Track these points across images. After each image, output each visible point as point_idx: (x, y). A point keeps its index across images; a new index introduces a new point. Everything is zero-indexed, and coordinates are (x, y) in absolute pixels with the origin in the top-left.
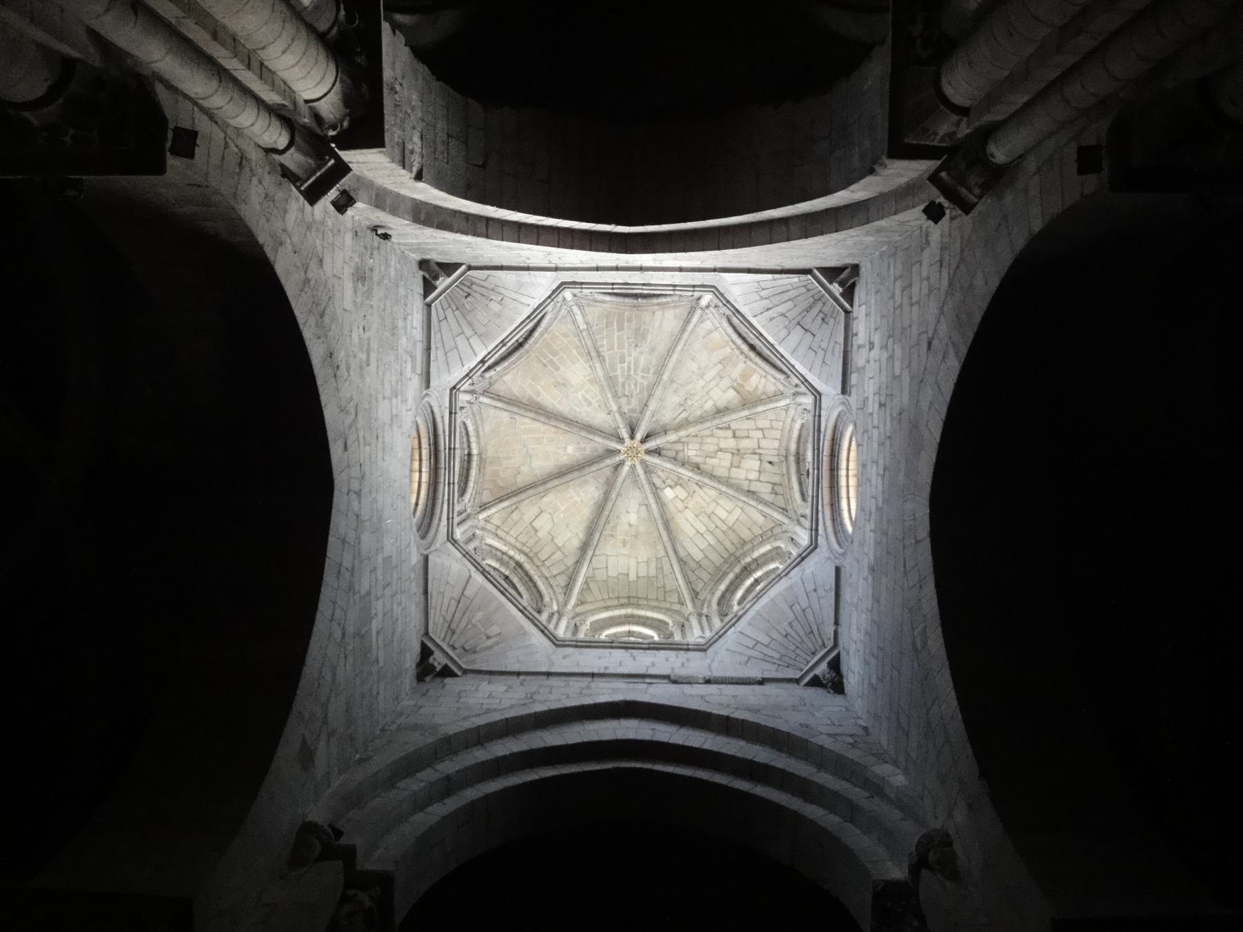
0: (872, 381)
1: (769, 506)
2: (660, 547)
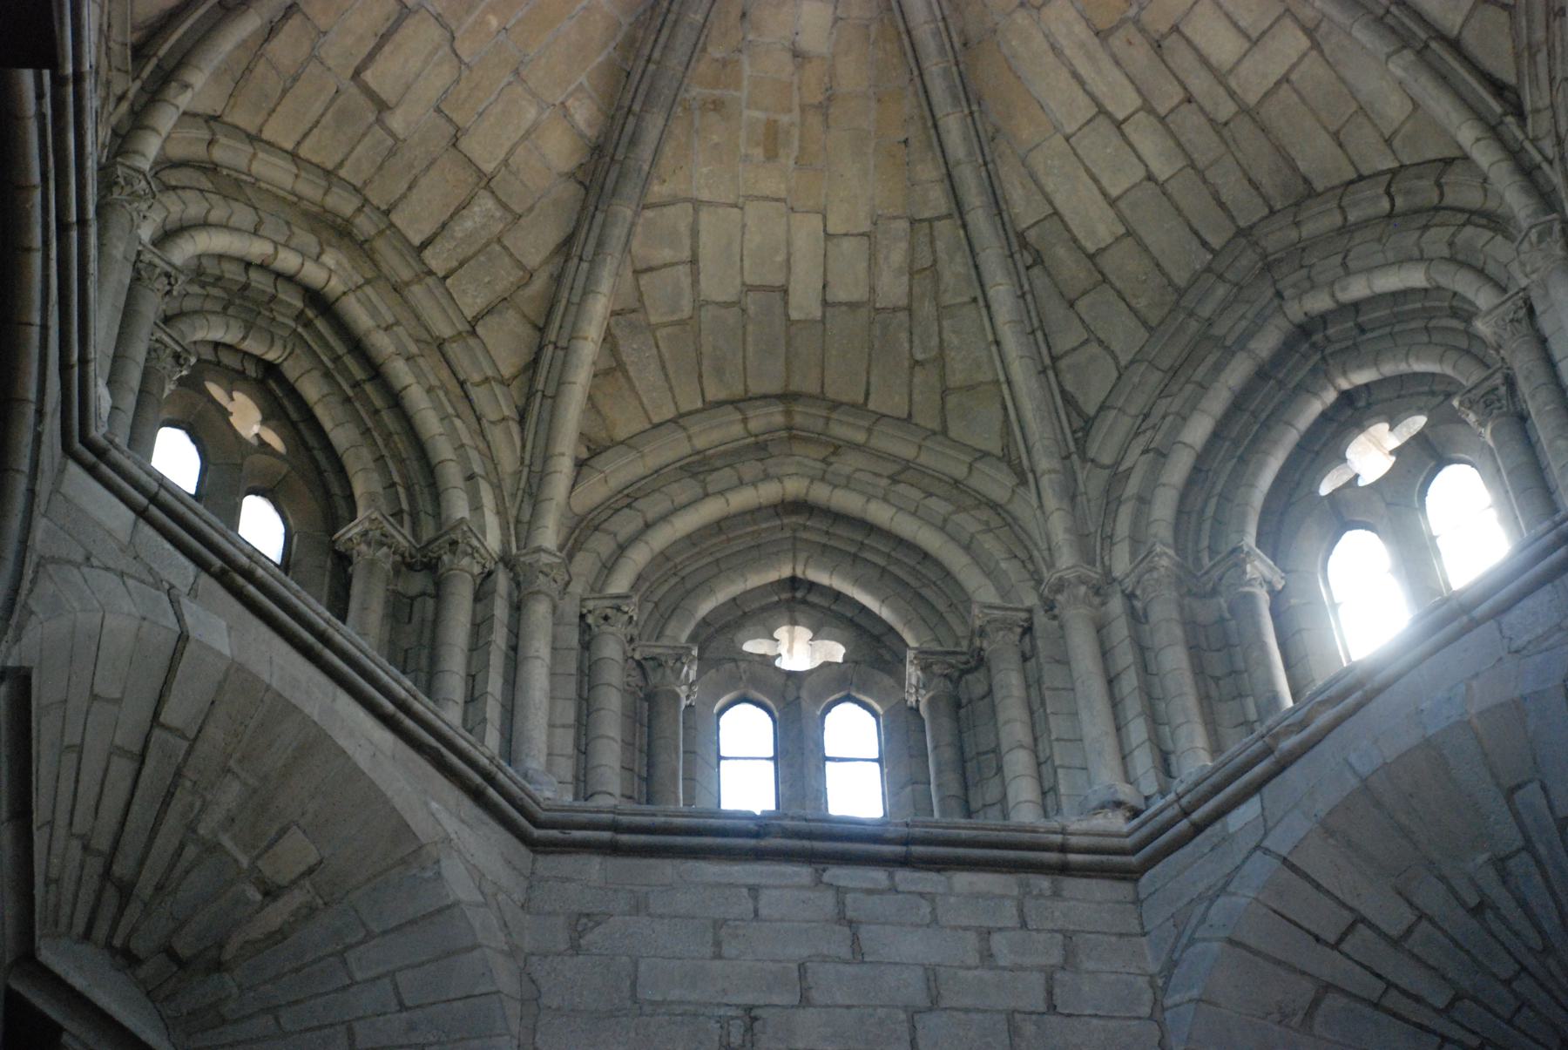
2: (928, 171)
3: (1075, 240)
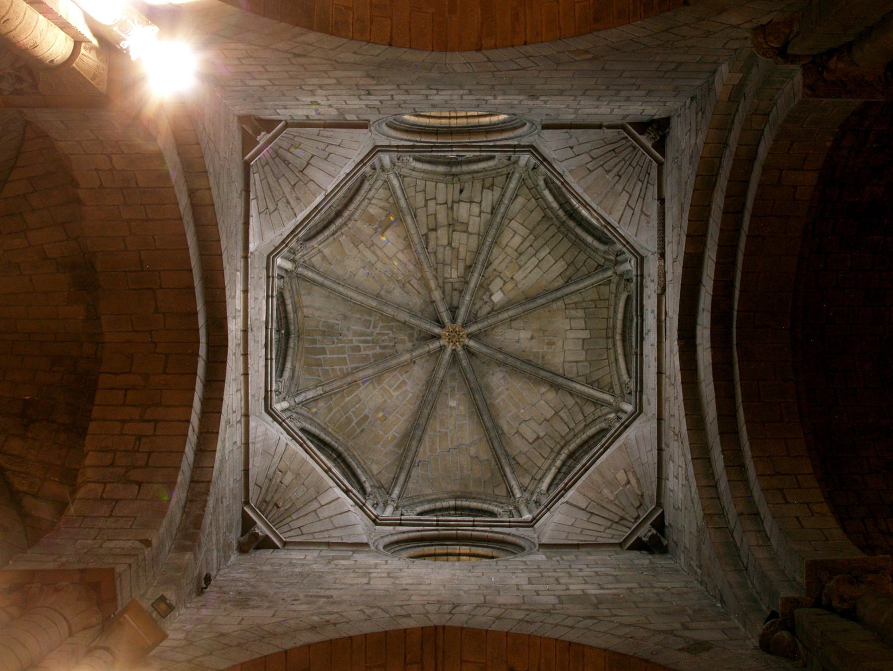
1: (505, 192)
2: (554, 306)
3: (565, 270)
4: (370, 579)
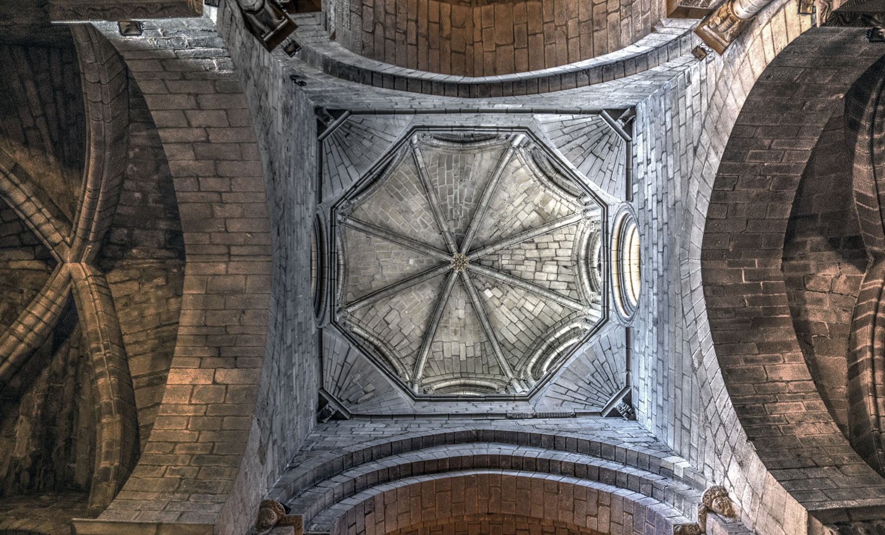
0: (650, 187)
1: (566, 298)
2: (483, 335)
4: (300, 205)
